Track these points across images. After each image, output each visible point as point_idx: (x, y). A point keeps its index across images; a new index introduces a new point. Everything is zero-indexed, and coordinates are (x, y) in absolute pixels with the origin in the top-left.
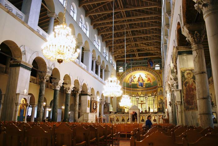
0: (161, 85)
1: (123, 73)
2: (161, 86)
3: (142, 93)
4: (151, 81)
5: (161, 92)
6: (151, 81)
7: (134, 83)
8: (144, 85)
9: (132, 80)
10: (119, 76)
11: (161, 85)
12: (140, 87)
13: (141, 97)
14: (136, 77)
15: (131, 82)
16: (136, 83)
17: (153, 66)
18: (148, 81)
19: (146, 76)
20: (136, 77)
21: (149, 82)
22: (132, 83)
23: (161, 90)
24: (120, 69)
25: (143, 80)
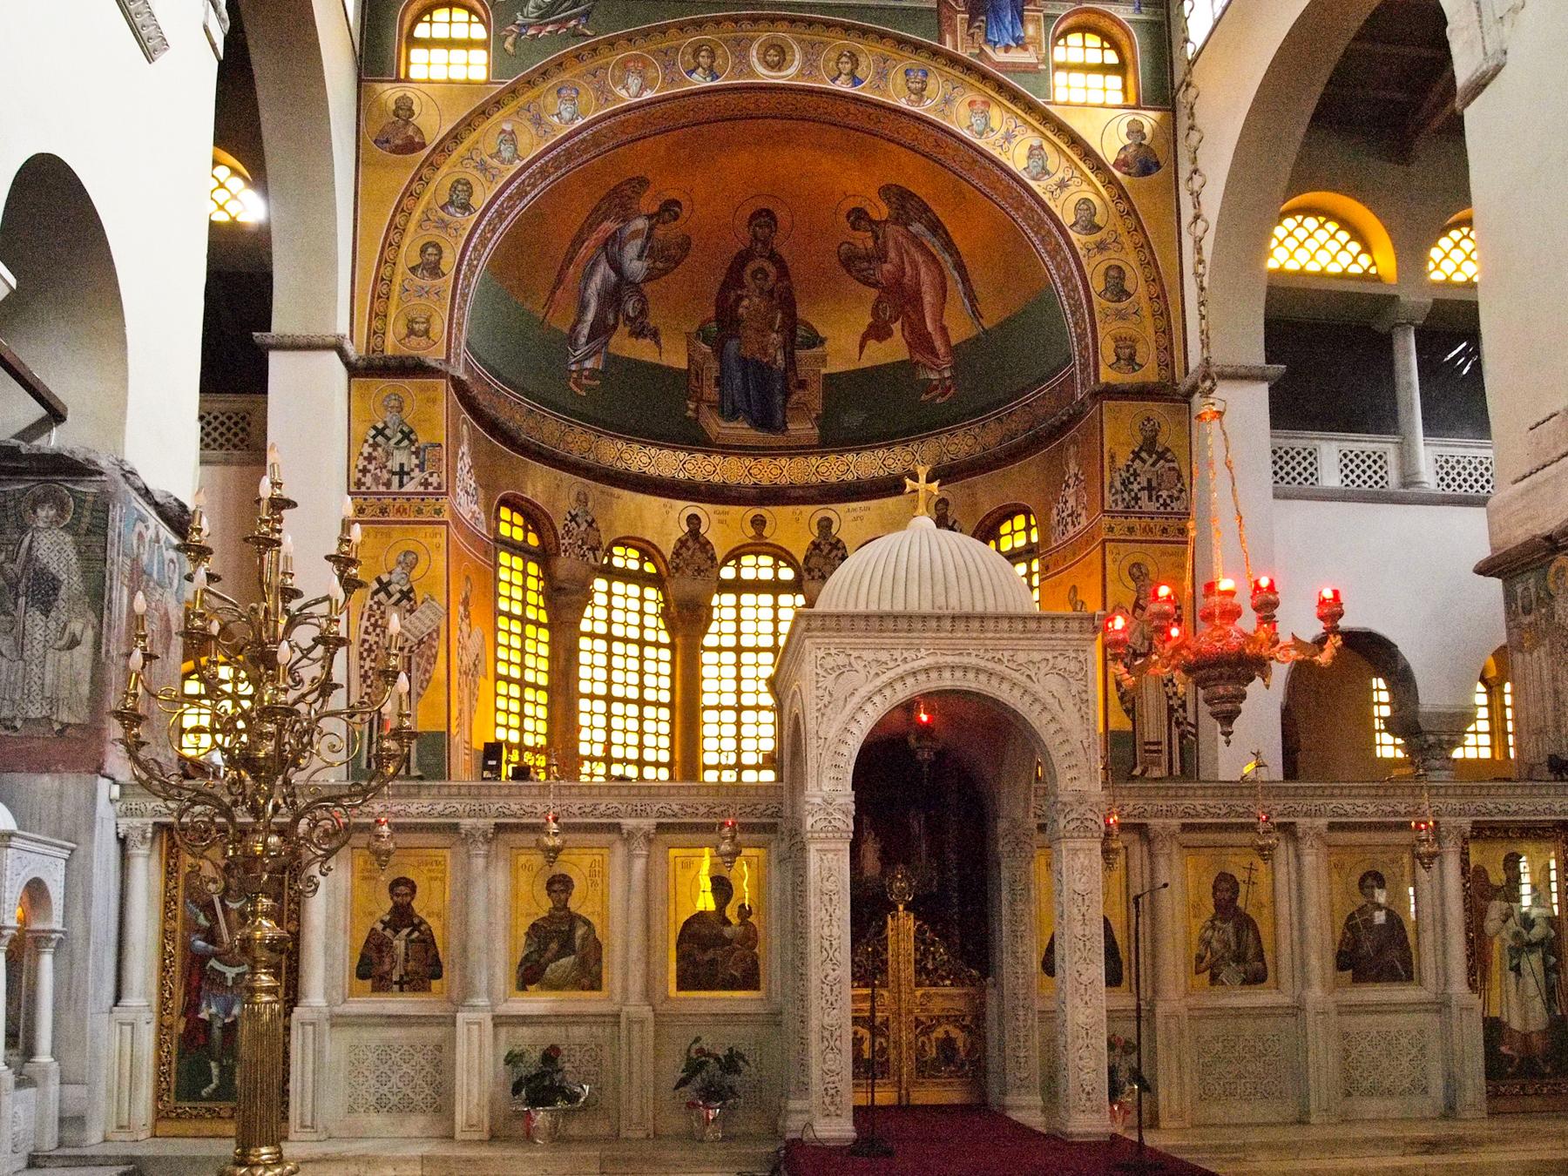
0: (1147, 354)
1: (497, 103)
2: (1149, 373)
3: (759, 522)
4: (920, 340)
5: (1145, 470)
6: (920, 340)
7: (642, 351)
8: (802, 407)
9: (613, 297)
10: (411, 147)
11: (1147, 354)
12: (740, 430)
13: (739, 586)
14: (685, 245)
15: (601, 330)
16: (676, 358)
17: (1021, 43)
18: (878, 331)
19: (864, 241)
20: (685, 245)
21: (893, 349)
22: (625, 345)
23: (1149, 444)
24: (430, 43)
25: (791, 323)
